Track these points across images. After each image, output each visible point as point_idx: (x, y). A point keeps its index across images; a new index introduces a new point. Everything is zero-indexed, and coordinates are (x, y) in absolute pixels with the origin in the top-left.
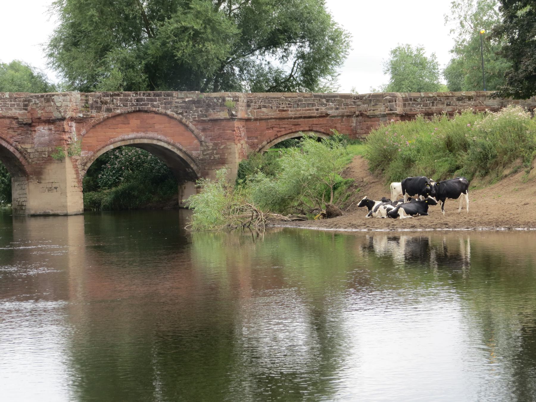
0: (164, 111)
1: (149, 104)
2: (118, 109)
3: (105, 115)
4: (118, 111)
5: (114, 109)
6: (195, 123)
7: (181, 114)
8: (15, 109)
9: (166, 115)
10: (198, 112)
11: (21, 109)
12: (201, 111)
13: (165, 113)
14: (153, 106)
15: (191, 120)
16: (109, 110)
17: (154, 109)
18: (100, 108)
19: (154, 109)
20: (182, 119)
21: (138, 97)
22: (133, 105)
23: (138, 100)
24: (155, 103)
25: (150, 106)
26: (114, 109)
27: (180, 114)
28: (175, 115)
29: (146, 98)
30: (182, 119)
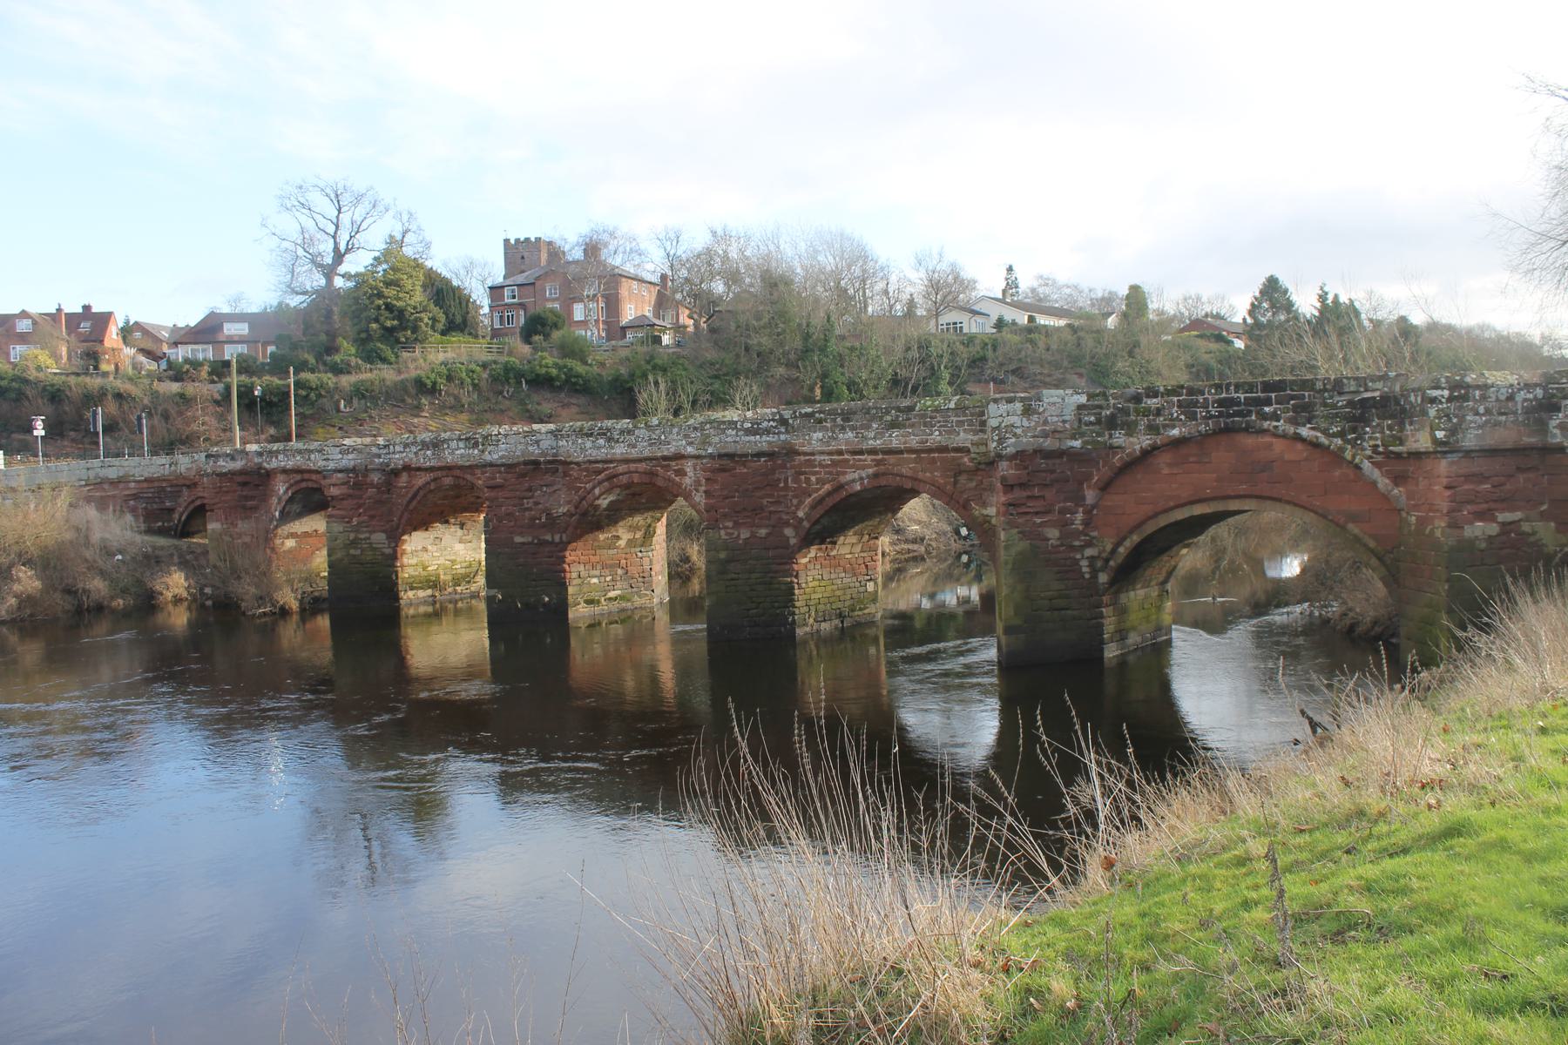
0: (1291, 429)
1: (1251, 411)
2: (1174, 427)
3: (1142, 441)
4: (1175, 432)
5: (1165, 426)
6: (1379, 458)
7: (1341, 434)
8: (965, 430)
9: (1298, 438)
10: (1382, 432)
11: (976, 432)
12: (1390, 428)
13: (1295, 433)
14: (1265, 417)
15: (1369, 452)
16: (1153, 429)
17: (1266, 424)
18: (1136, 423)
19: (1266, 424)
20: (1342, 449)
21: (1224, 395)
22: (1212, 417)
23: (1221, 403)
24: (1267, 409)
25: (1253, 417)
26: (1165, 426)
27: (1334, 435)
28: (1324, 440)
29: (1242, 396)
30: (1342, 449)
